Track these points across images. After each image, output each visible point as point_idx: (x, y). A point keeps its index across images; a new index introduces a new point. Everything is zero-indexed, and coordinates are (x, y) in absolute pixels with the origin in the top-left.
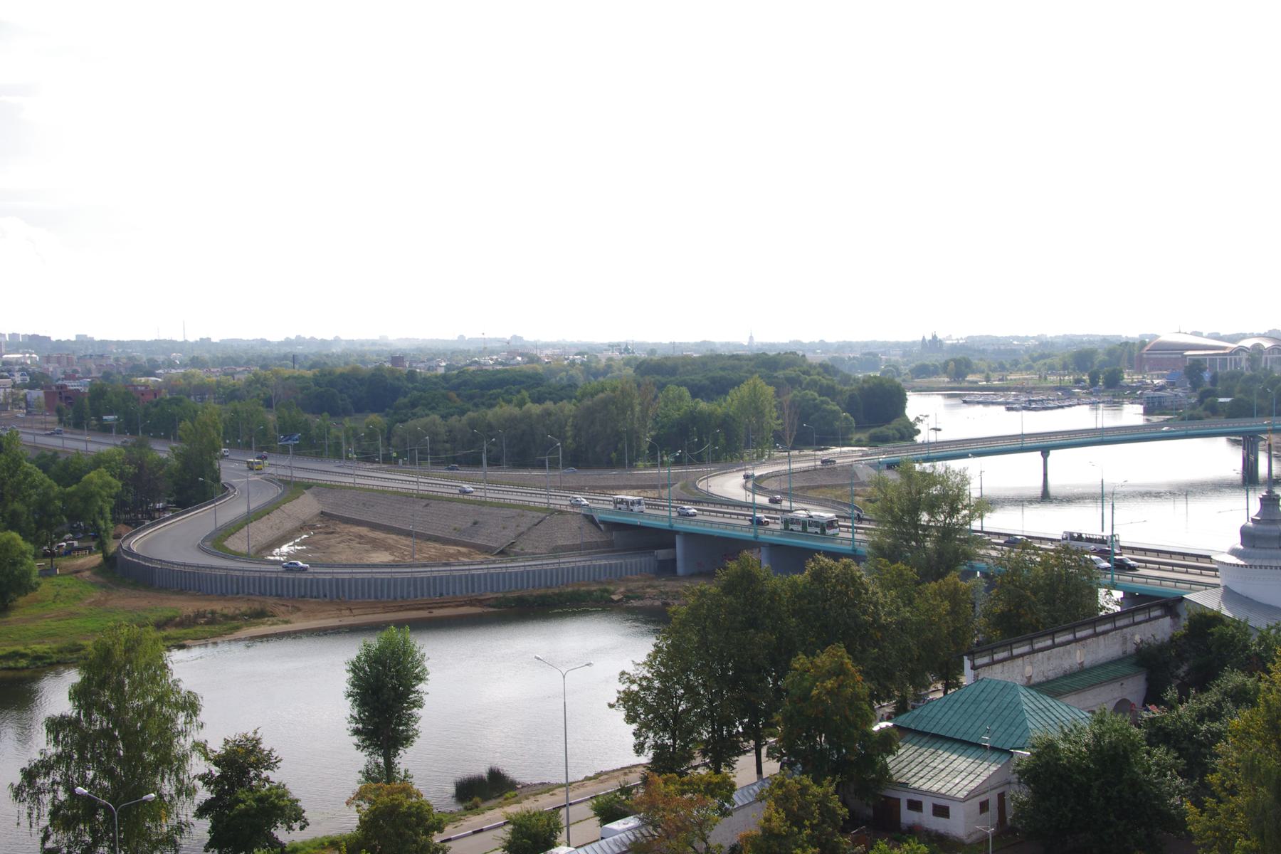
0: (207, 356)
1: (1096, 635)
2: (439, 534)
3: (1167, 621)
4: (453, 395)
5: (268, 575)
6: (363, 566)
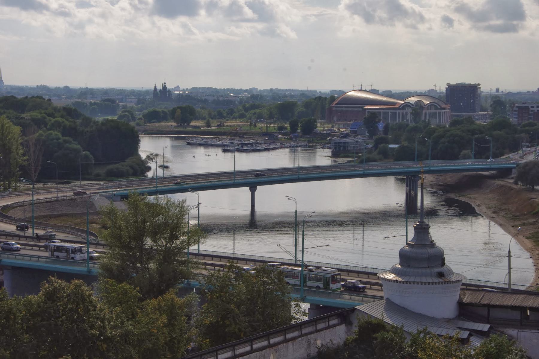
1: (286, 341)
3: (343, 328)
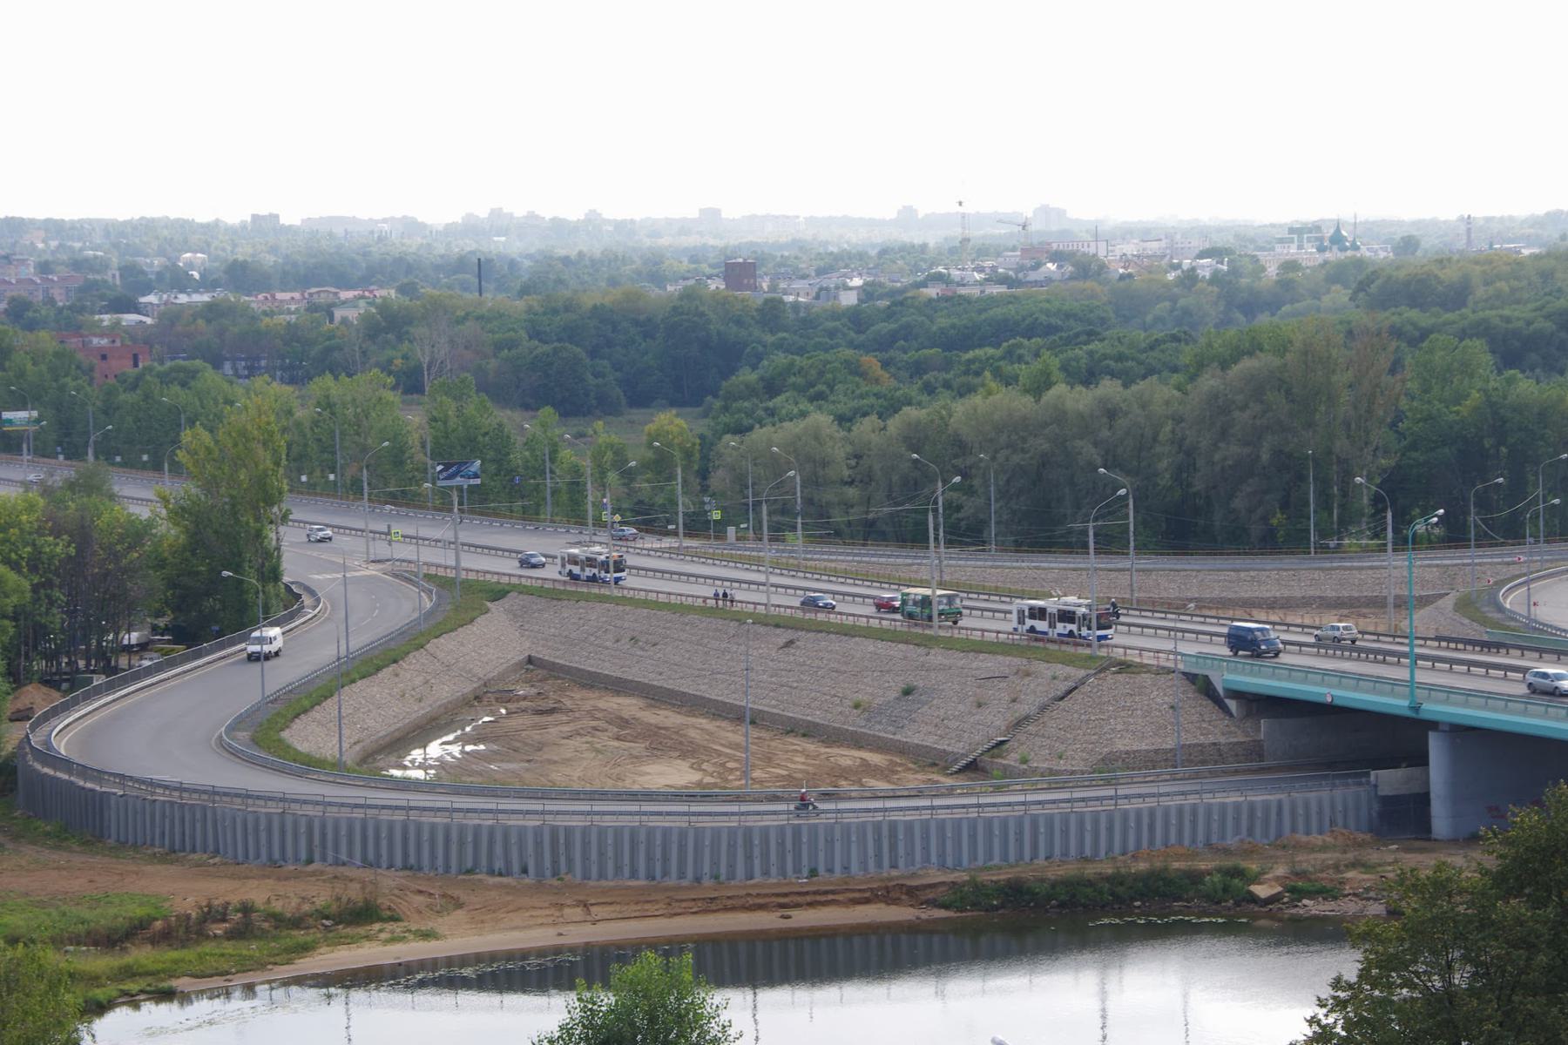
0: (269, 260)
2: (817, 717)
4: (871, 362)
5: (385, 816)
6: (619, 796)
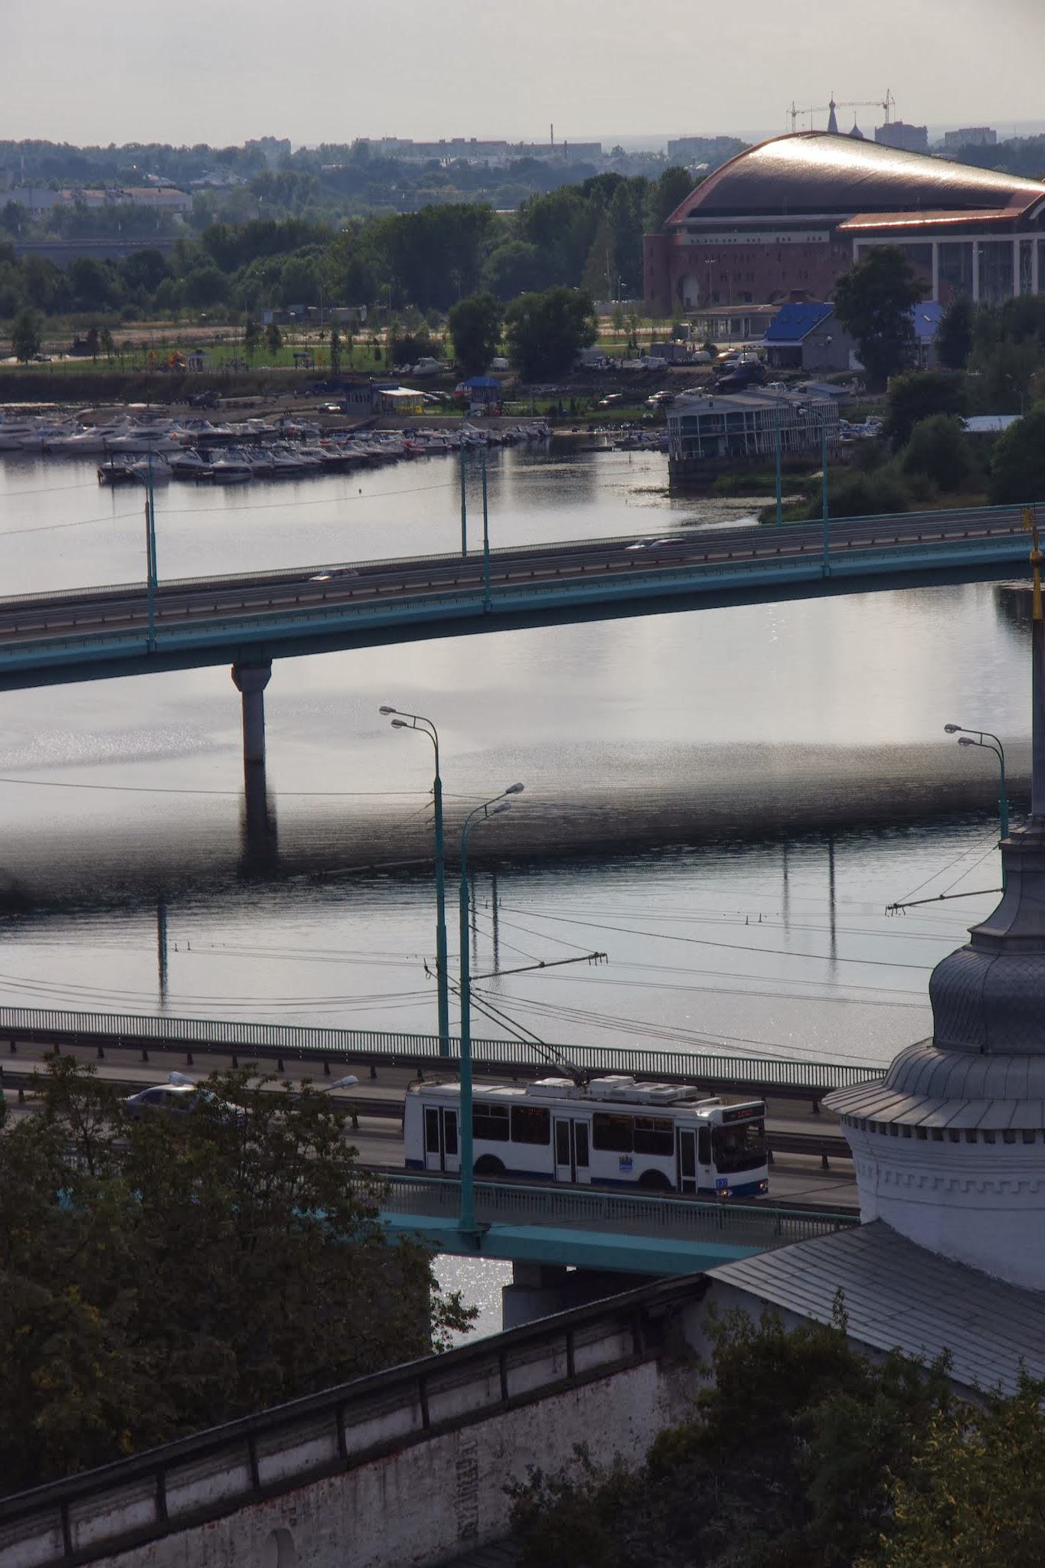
1: (346, 1463)
3: (646, 1380)
